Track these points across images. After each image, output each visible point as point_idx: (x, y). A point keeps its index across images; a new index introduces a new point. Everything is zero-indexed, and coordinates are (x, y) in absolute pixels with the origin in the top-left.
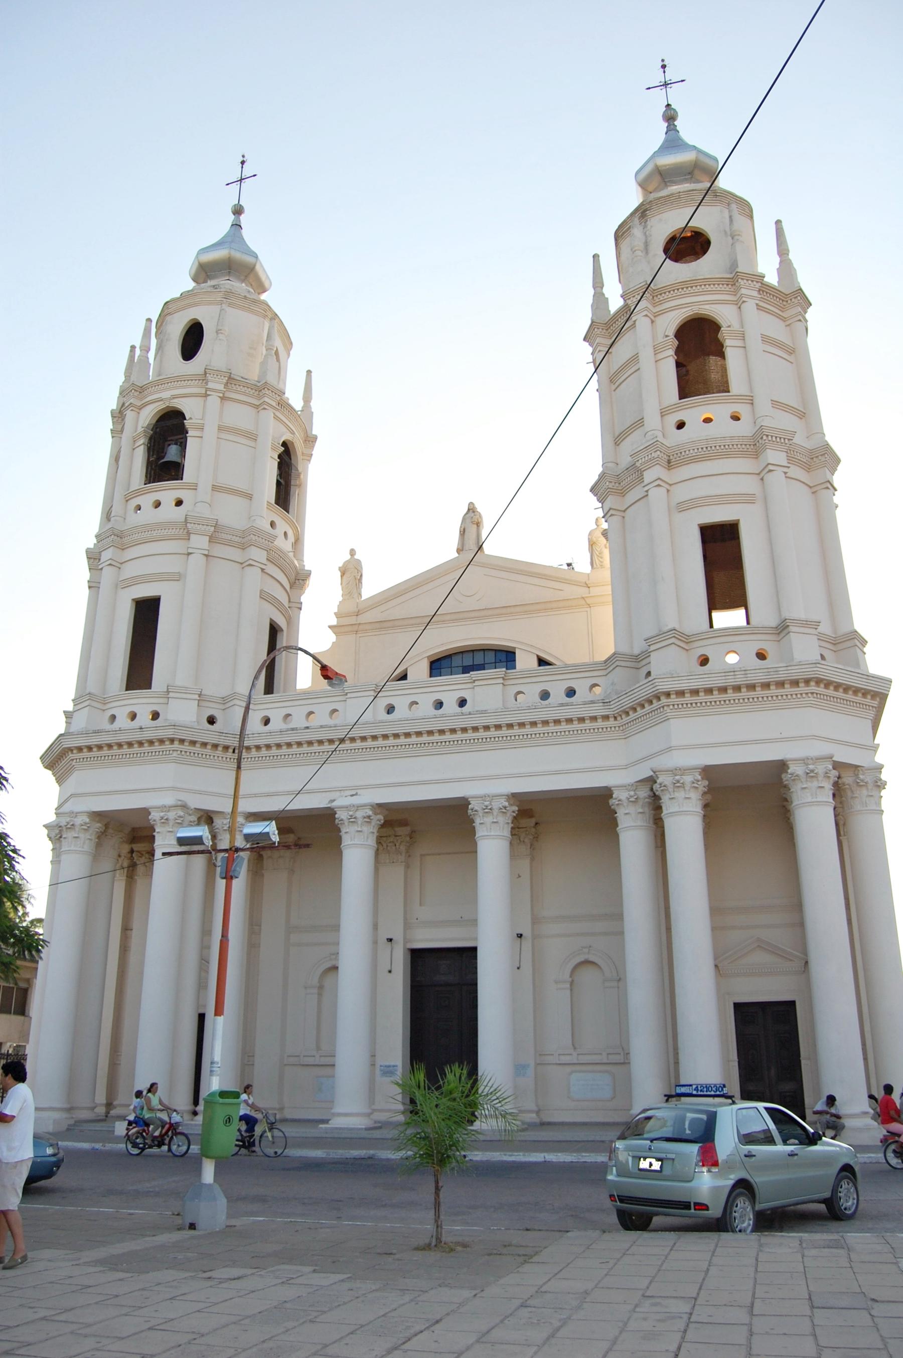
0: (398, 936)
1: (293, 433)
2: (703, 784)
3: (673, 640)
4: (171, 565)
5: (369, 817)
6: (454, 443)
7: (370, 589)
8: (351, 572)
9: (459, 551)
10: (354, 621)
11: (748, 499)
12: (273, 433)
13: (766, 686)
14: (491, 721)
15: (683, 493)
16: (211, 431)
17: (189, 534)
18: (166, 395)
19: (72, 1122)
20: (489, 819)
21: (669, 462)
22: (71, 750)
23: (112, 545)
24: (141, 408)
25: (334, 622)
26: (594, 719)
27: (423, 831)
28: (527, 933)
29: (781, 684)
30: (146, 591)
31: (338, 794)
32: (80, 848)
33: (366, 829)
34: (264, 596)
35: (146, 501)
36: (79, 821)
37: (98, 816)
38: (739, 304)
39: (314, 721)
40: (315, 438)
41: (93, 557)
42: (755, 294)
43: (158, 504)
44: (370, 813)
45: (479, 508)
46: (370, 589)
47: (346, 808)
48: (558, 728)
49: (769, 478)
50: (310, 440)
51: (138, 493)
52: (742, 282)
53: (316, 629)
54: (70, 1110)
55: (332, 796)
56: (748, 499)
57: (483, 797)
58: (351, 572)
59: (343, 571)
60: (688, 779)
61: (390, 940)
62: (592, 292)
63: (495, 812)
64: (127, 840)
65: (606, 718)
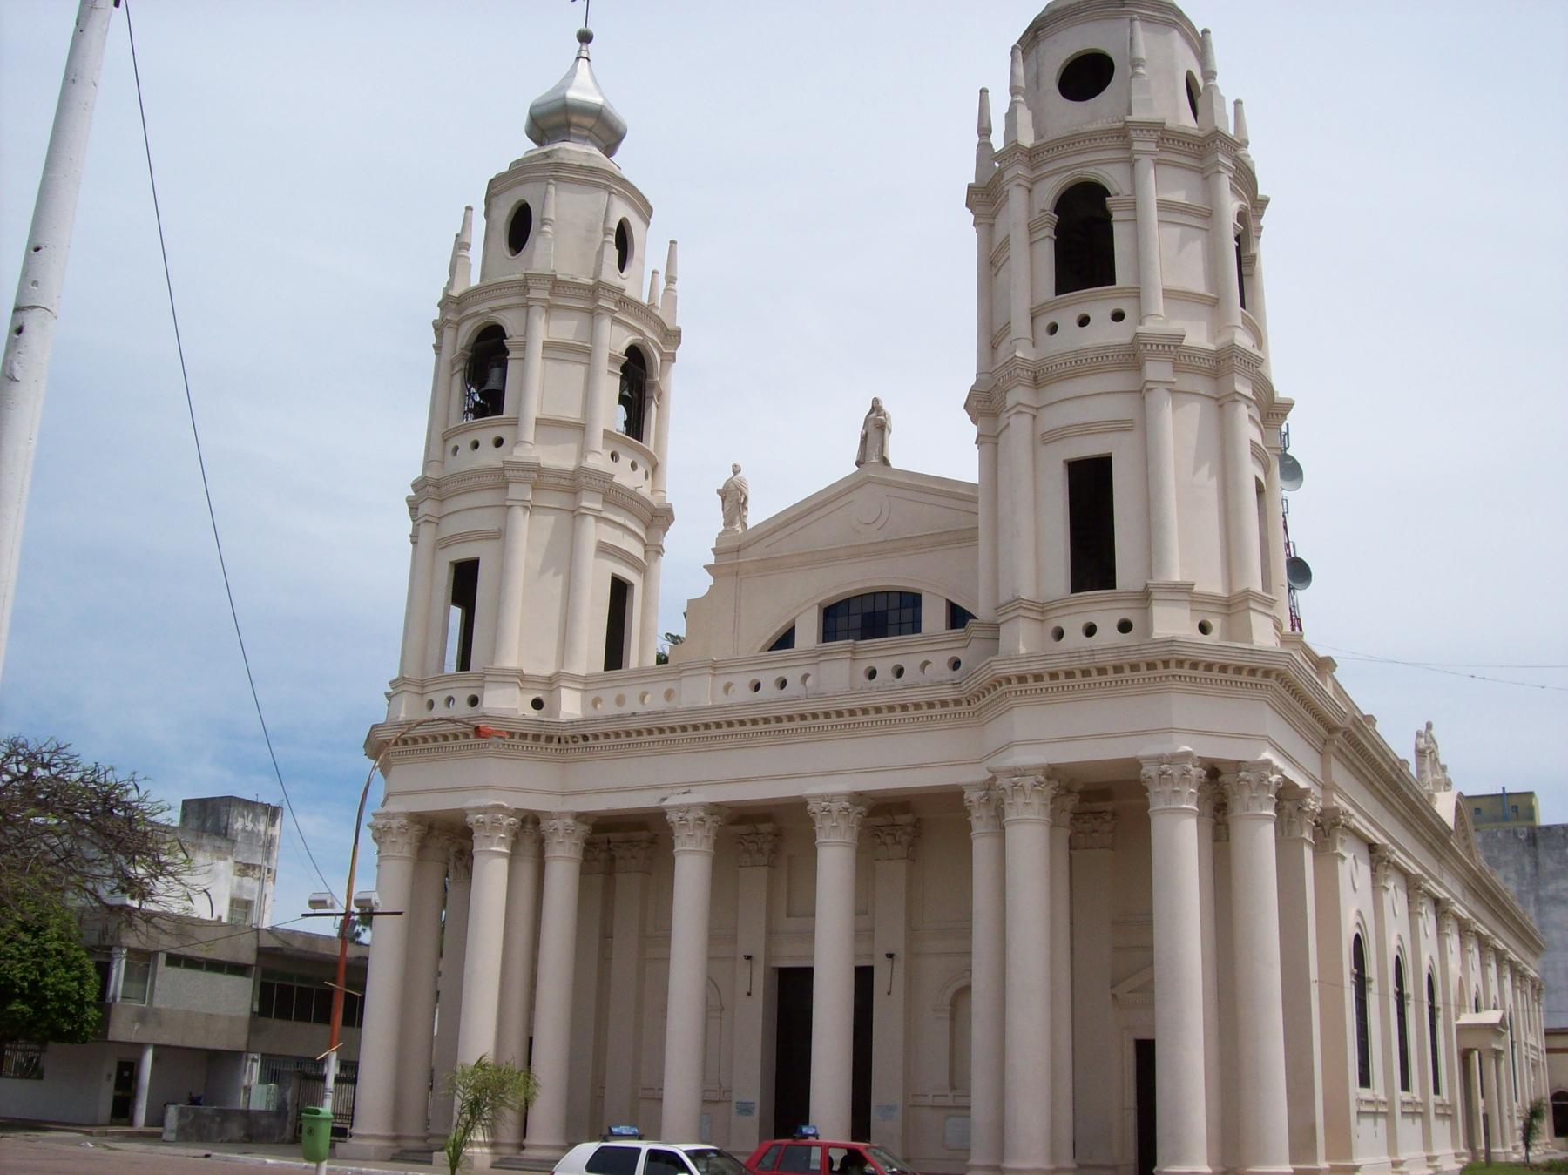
0: (759, 952)
1: (641, 333)
2: (1049, 791)
3: (1021, 612)
4: (485, 521)
5: (701, 819)
6: (827, 338)
7: (757, 515)
8: (733, 498)
9: (858, 464)
10: (738, 557)
11: (1121, 426)
12: (614, 340)
13: (1118, 669)
14: (831, 706)
15: (1054, 419)
16: (536, 350)
17: (507, 483)
18: (483, 308)
19: (397, 1151)
20: (828, 823)
21: (1035, 379)
22: (387, 742)
23: (429, 496)
24: (459, 324)
25: (711, 560)
26: (944, 704)
27: (763, 838)
28: (901, 953)
29: (1134, 667)
30: (464, 553)
31: (669, 791)
32: (403, 849)
33: (699, 833)
34: (605, 550)
35: (464, 442)
36: (395, 824)
37: (417, 818)
38: (1131, 163)
39: (627, 709)
40: (678, 333)
41: (413, 506)
42: (1153, 147)
43: (476, 445)
44: (702, 814)
45: (885, 406)
46: (757, 515)
47: (678, 808)
48: (892, 716)
49: (1150, 398)
50: (672, 337)
51: (457, 431)
52: (1133, 134)
53: (682, 571)
54: (396, 1138)
55: (661, 793)
56: (1121, 426)
57: (822, 797)
58: (733, 498)
59: (724, 493)
60: (1028, 782)
61: (749, 957)
62: (977, 139)
63: (835, 814)
64: (444, 844)
65: (957, 702)
